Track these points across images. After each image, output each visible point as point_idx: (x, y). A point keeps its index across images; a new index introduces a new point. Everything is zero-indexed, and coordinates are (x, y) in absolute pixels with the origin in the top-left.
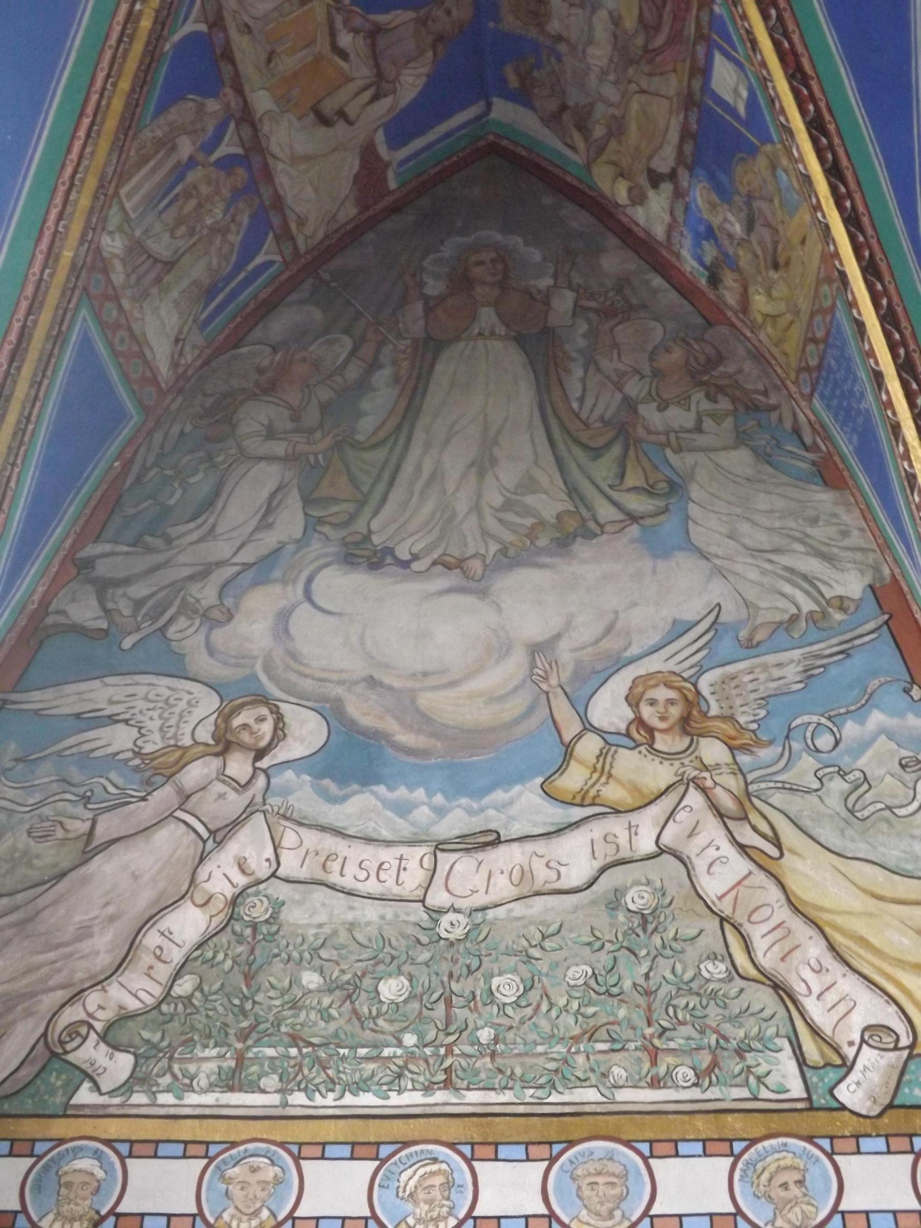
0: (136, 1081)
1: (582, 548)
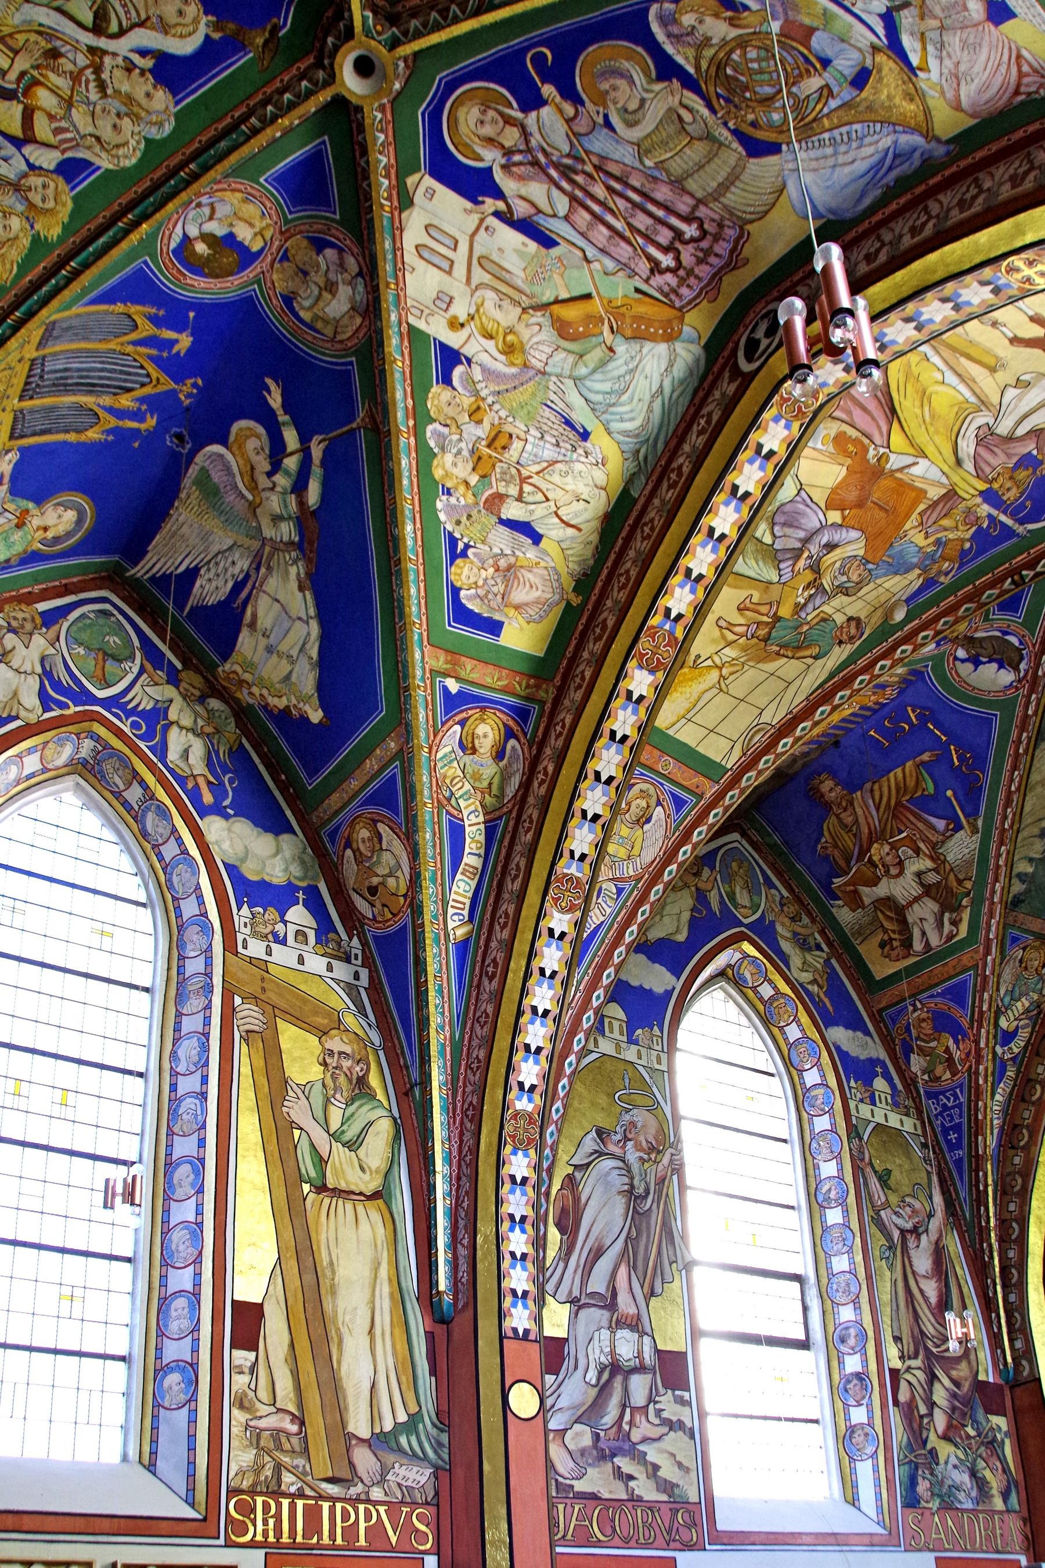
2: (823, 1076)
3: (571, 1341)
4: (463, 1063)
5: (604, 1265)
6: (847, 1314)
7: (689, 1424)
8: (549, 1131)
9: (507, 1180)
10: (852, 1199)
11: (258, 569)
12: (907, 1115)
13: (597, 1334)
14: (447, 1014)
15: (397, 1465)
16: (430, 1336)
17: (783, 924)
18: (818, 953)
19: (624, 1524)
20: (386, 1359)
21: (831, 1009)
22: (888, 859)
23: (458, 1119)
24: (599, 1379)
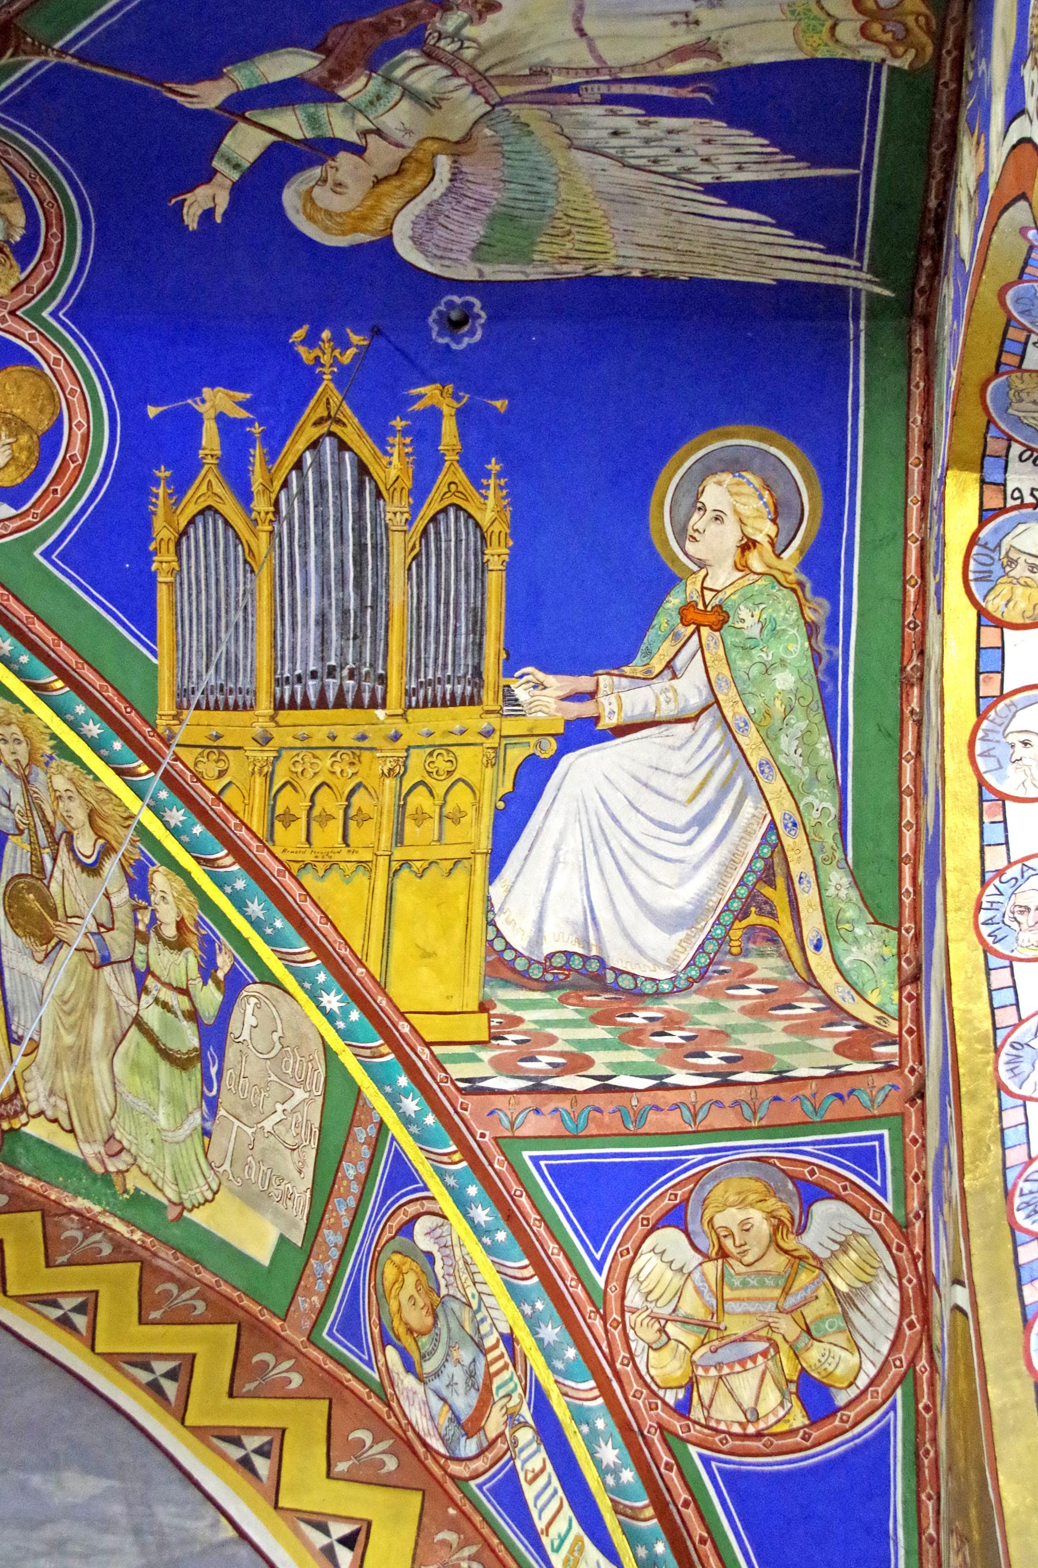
11: (574, 88)
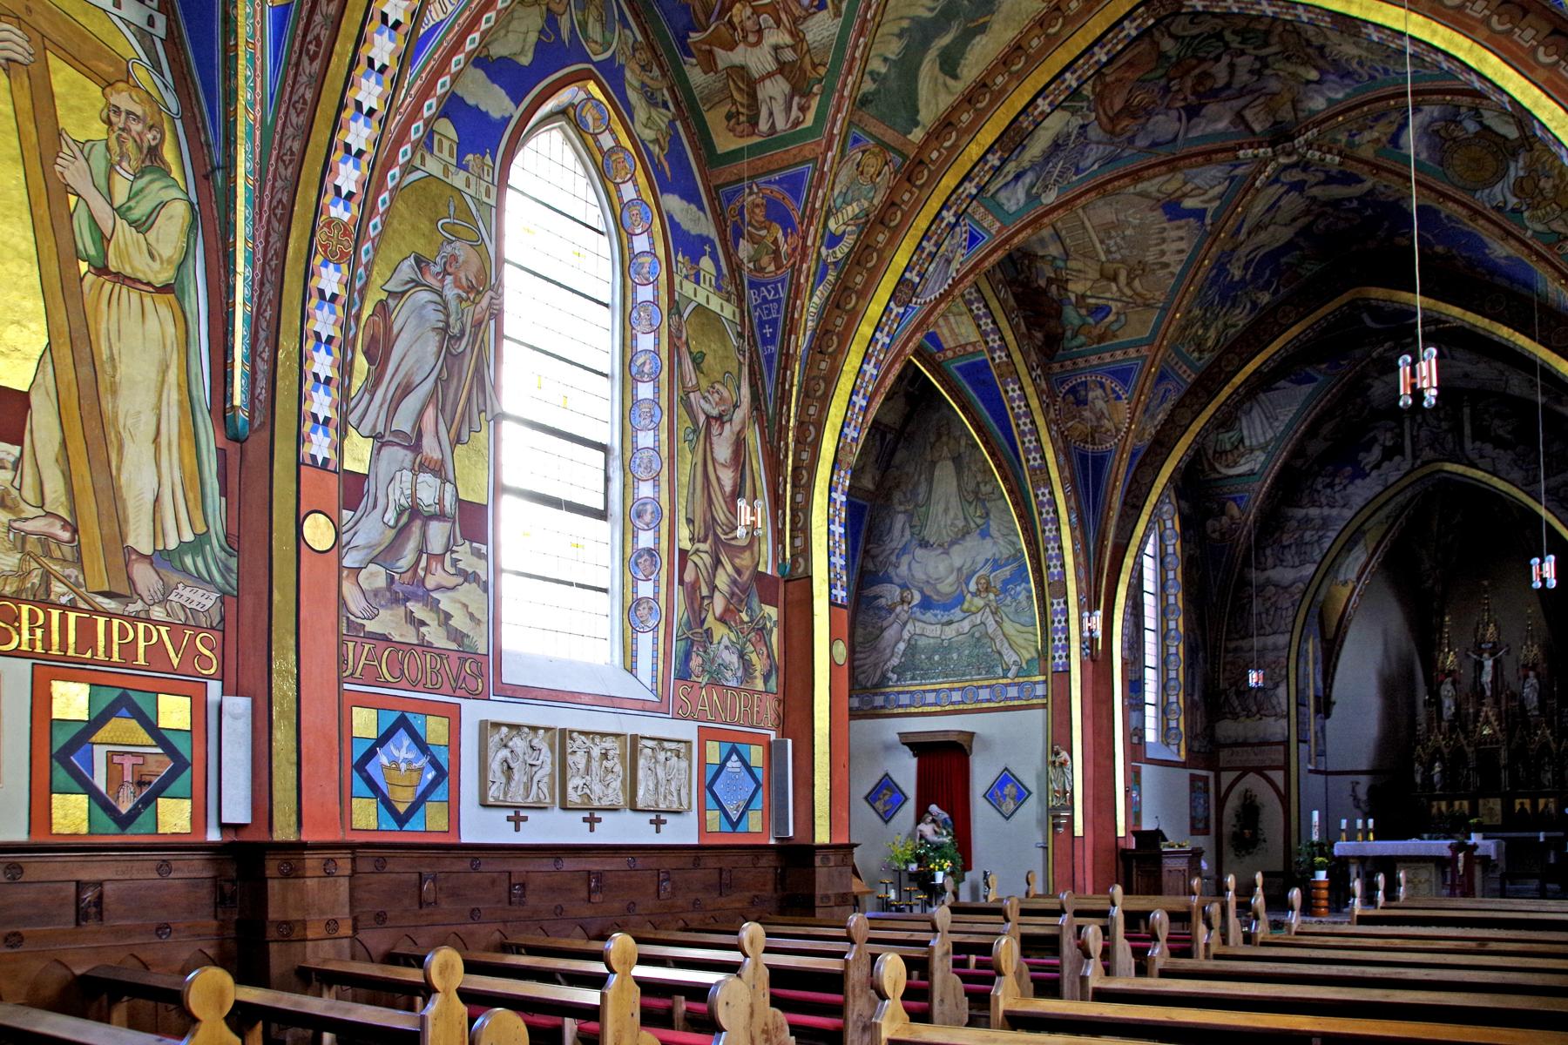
0: (898, 680)
1: (968, 538)
2: (652, 244)
3: (372, 477)
4: (275, 153)
5: (411, 404)
6: (646, 490)
7: (484, 578)
8: (364, 248)
9: (315, 294)
10: (664, 375)
12: (728, 300)
13: (398, 474)
14: (258, 90)
15: (180, 586)
16: (222, 454)
17: (633, 71)
18: (664, 111)
19: (413, 667)
20: (172, 473)
21: (669, 174)
22: (749, 24)
23: (265, 216)
24: (397, 521)
